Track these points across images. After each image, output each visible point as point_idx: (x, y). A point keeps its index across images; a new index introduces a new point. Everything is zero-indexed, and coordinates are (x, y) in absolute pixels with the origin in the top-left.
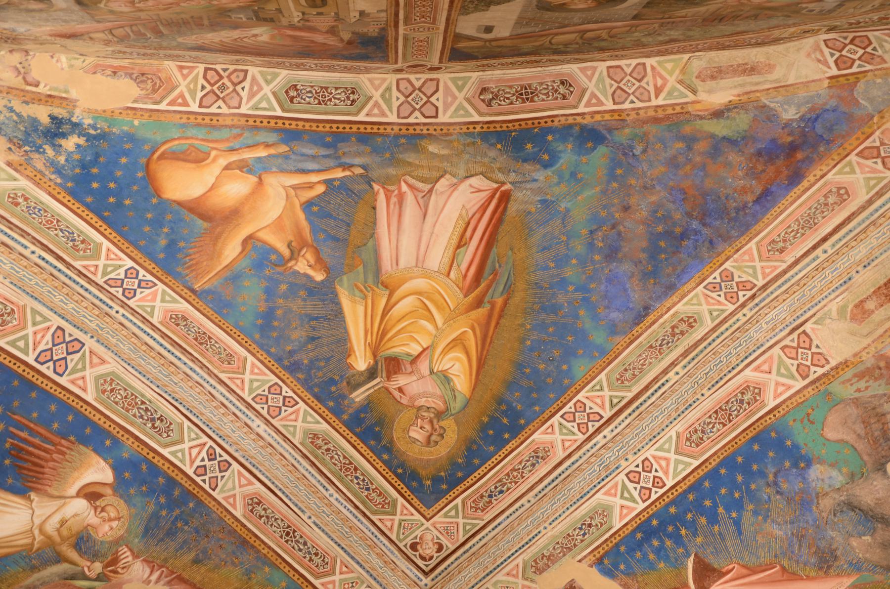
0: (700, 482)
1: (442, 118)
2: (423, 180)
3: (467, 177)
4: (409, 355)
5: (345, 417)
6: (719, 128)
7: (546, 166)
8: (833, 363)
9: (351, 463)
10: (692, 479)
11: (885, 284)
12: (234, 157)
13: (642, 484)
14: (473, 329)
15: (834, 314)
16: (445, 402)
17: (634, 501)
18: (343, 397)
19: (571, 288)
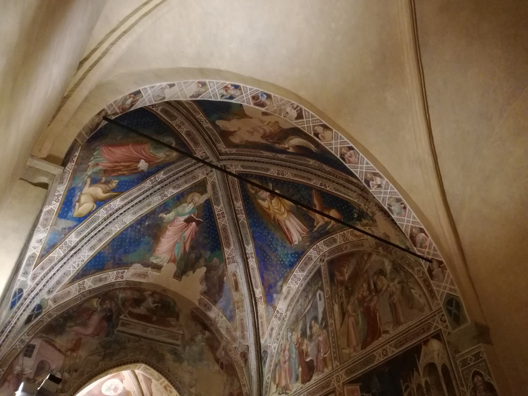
0: (216, 227)
1: (312, 250)
2: (304, 237)
3: (299, 242)
4: (273, 200)
5: (268, 178)
6: (279, 284)
7: (291, 254)
8: (228, 265)
9: (257, 169)
10: (217, 226)
11: (237, 282)
12: (331, 224)
13: (221, 215)
14: (270, 213)
15: (236, 270)
16: (259, 195)
17: (218, 212)
18: (272, 183)
19: (267, 234)
